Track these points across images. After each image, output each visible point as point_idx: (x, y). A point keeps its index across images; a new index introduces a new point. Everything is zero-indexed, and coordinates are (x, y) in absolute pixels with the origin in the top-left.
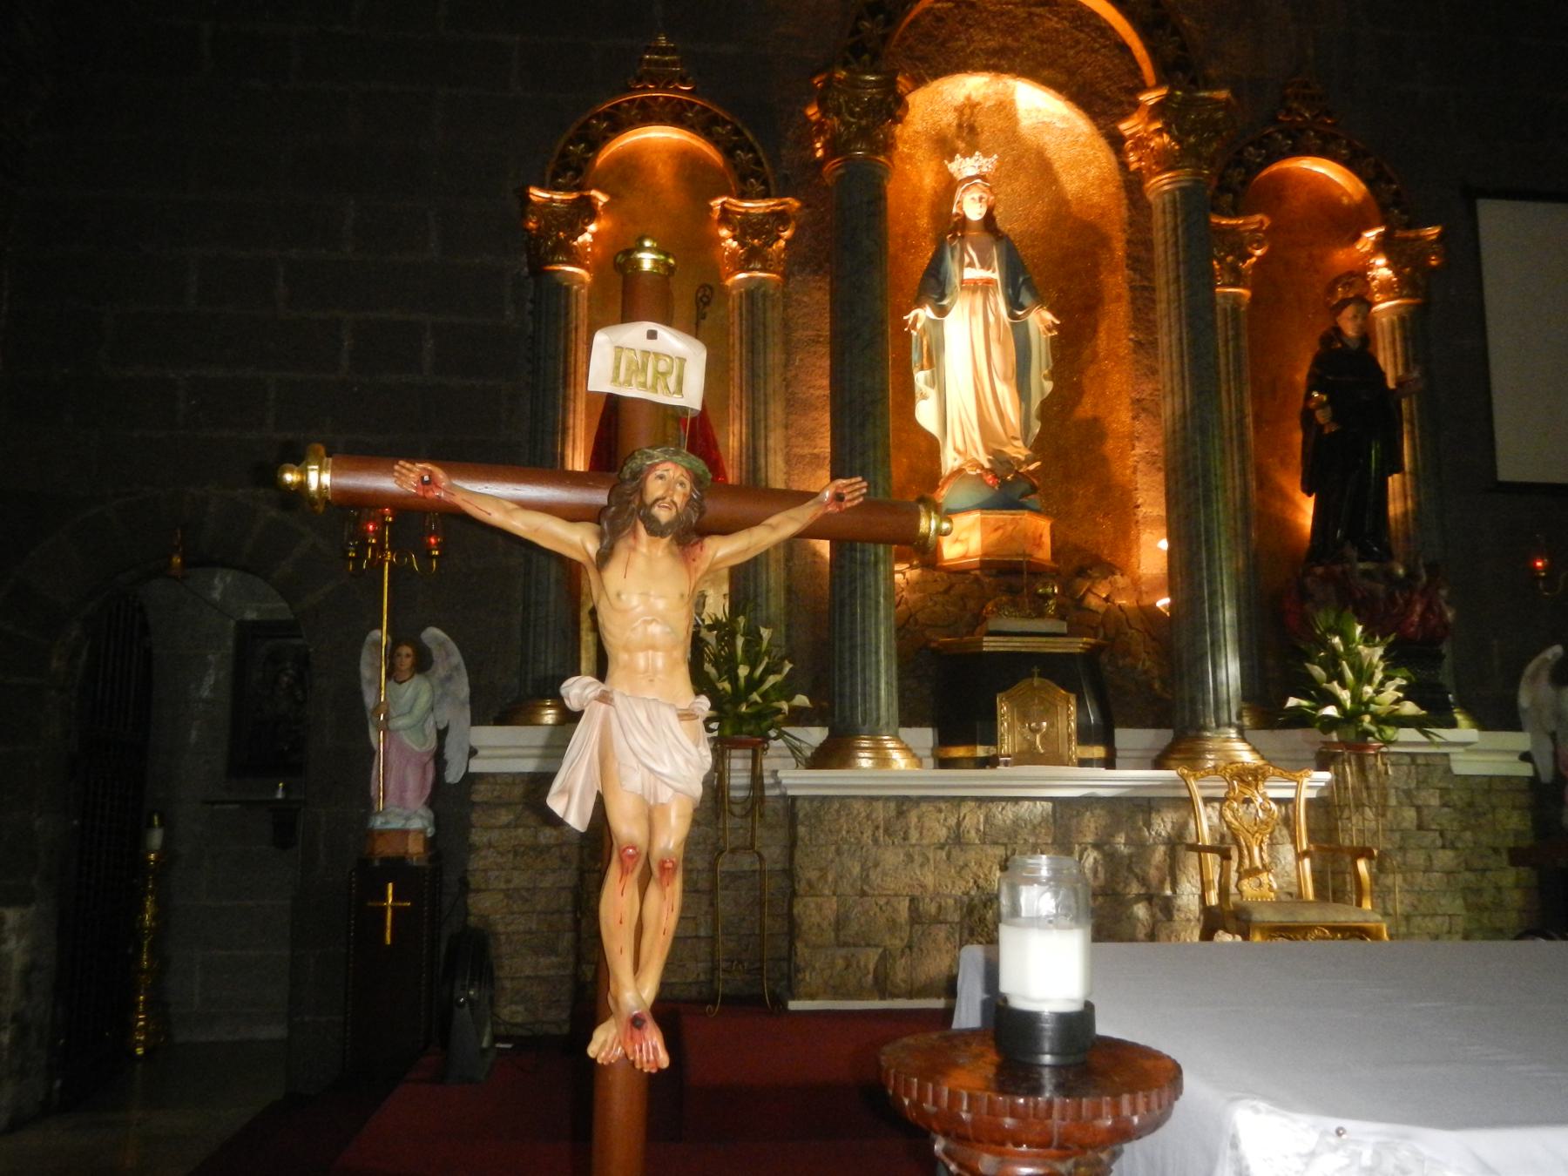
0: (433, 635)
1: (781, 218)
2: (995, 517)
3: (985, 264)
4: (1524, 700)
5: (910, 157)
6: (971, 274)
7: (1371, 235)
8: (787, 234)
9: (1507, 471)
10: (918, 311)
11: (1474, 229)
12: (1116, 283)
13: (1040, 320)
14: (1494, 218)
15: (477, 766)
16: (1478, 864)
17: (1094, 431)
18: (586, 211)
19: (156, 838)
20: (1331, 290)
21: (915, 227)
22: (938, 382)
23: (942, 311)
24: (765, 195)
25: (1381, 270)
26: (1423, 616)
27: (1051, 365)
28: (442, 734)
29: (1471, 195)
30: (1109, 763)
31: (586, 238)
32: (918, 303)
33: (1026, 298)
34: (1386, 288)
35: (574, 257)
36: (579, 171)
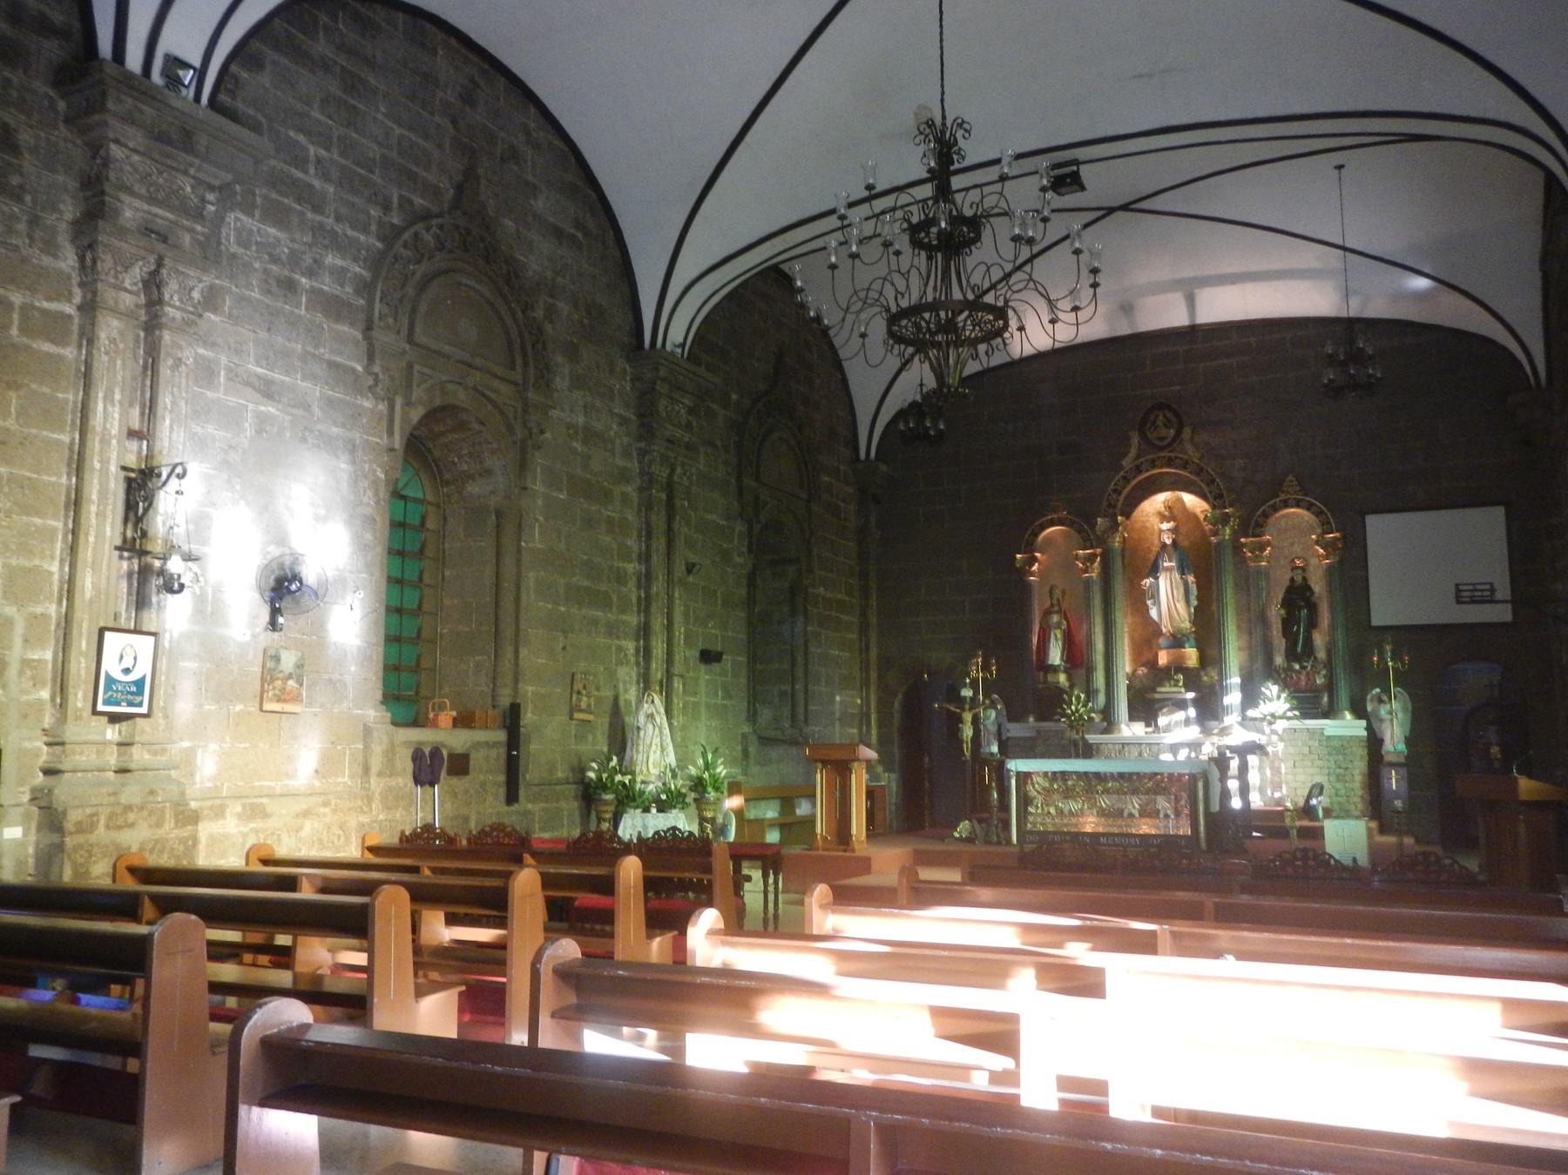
2: (1172, 651)
3: (1170, 561)
4: (1369, 708)
5: (1148, 521)
6: (1165, 564)
7: (1313, 537)
8: (1098, 559)
9: (1377, 620)
10: (1147, 580)
13: (1191, 578)
14: (1372, 521)
15: (1009, 735)
16: (1344, 766)
18: (1035, 560)
19: (927, 760)
21: (1152, 544)
22: (1157, 603)
23: (1157, 578)
25: (1321, 551)
26: (1307, 683)
28: (1000, 726)
29: (1363, 515)
31: (1035, 568)
33: (1186, 571)
34: (1322, 556)
36: (1032, 544)
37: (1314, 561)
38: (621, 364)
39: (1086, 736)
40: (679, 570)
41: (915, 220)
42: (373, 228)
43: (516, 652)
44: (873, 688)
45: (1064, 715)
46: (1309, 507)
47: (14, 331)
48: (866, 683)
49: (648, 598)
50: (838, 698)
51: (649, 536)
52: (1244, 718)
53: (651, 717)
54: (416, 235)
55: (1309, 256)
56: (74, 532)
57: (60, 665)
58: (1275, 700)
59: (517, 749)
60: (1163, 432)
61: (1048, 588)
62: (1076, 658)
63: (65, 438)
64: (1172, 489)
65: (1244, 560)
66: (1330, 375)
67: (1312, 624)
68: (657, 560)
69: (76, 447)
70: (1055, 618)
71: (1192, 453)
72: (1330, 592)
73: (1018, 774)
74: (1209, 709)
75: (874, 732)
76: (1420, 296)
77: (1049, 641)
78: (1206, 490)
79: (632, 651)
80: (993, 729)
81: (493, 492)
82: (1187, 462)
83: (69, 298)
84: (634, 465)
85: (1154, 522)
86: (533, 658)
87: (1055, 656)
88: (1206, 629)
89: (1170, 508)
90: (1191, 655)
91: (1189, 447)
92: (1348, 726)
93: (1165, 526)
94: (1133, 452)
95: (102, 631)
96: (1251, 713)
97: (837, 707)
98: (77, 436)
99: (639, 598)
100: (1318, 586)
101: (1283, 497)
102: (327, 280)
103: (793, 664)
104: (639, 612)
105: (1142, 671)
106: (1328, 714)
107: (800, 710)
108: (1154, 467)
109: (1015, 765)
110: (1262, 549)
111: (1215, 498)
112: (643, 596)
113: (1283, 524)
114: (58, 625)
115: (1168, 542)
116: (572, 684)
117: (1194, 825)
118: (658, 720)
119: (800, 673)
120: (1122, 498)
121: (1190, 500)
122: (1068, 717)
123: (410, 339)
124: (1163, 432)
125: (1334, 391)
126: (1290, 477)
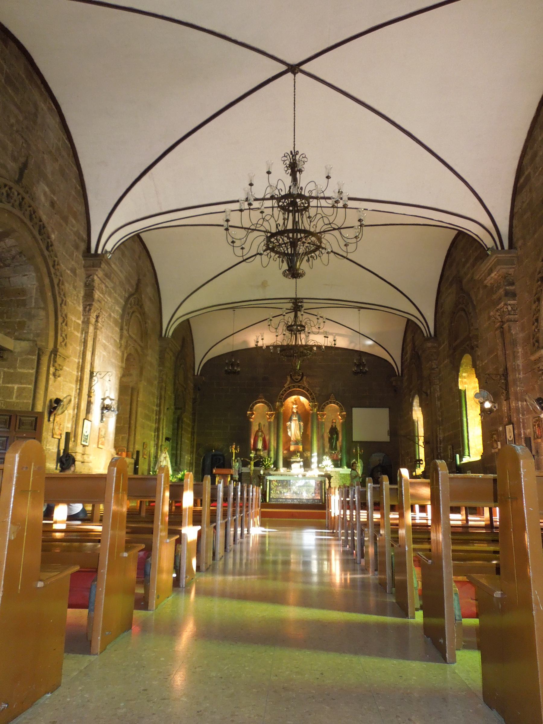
0: (239, 458)
1: (273, 414)
3: (296, 417)
6: (294, 418)
9: (354, 440)
11: (352, 411)
12: (310, 418)
13: (302, 423)
17: (308, 435)
18: (253, 414)
20: (332, 420)
22: (291, 430)
23: (291, 422)
24: (272, 411)
25: (340, 417)
27: (303, 428)
29: (352, 407)
30: (305, 471)
31: (253, 416)
32: (288, 422)
35: (252, 418)
37: (338, 420)
38: (158, 342)
39: (270, 472)
40: (166, 409)
41: (289, 324)
42: (123, 298)
43: (135, 434)
44: (194, 454)
45: (264, 465)
46: (337, 404)
47: (72, 329)
48: (192, 452)
49: (159, 419)
50: (186, 457)
51: (161, 398)
52: (318, 467)
53: (165, 458)
54: (131, 301)
55: (344, 330)
56: (80, 389)
57: (74, 429)
58: (327, 462)
59: (138, 465)
60: (297, 377)
61: (257, 423)
62: (266, 446)
63: (77, 360)
64: (298, 395)
65: (318, 419)
66: (354, 369)
67: (337, 439)
68: (162, 407)
69: (81, 364)
70: (260, 434)
71: (306, 384)
72: (342, 430)
73: (270, 481)
74: (307, 465)
75: (194, 469)
76: (370, 346)
77: (258, 441)
78: (310, 397)
79: (153, 436)
80: (237, 469)
81: (131, 381)
82: (304, 387)
83: (79, 319)
84: (157, 374)
85: (290, 405)
86: (138, 437)
87: (260, 446)
88: (306, 440)
89: (296, 401)
90: (301, 448)
91: (305, 382)
92: (345, 470)
93: (295, 406)
94: (288, 382)
95: (84, 420)
96: (320, 465)
97: (186, 460)
98: (81, 360)
99: (156, 419)
100: (339, 428)
101: (330, 400)
102: (115, 314)
103: (177, 444)
104: (156, 423)
105: (285, 452)
106: (341, 466)
107: (179, 460)
108: (294, 388)
109: (269, 478)
110: (323, 415)
111: (312, 399)
112: (157, 418)
113: (329, 409)
114: (73, 417)
115: (295, 411)
116: (143, 446)
117: (321, 497)
118: (167, 459)
119: (179, 447)
120: (284, 396)
121: (303, 399)
122: (265, 466)
123: (128, 333)
124: (297, 377)
125: (356, 373)
126: (332, 395)
